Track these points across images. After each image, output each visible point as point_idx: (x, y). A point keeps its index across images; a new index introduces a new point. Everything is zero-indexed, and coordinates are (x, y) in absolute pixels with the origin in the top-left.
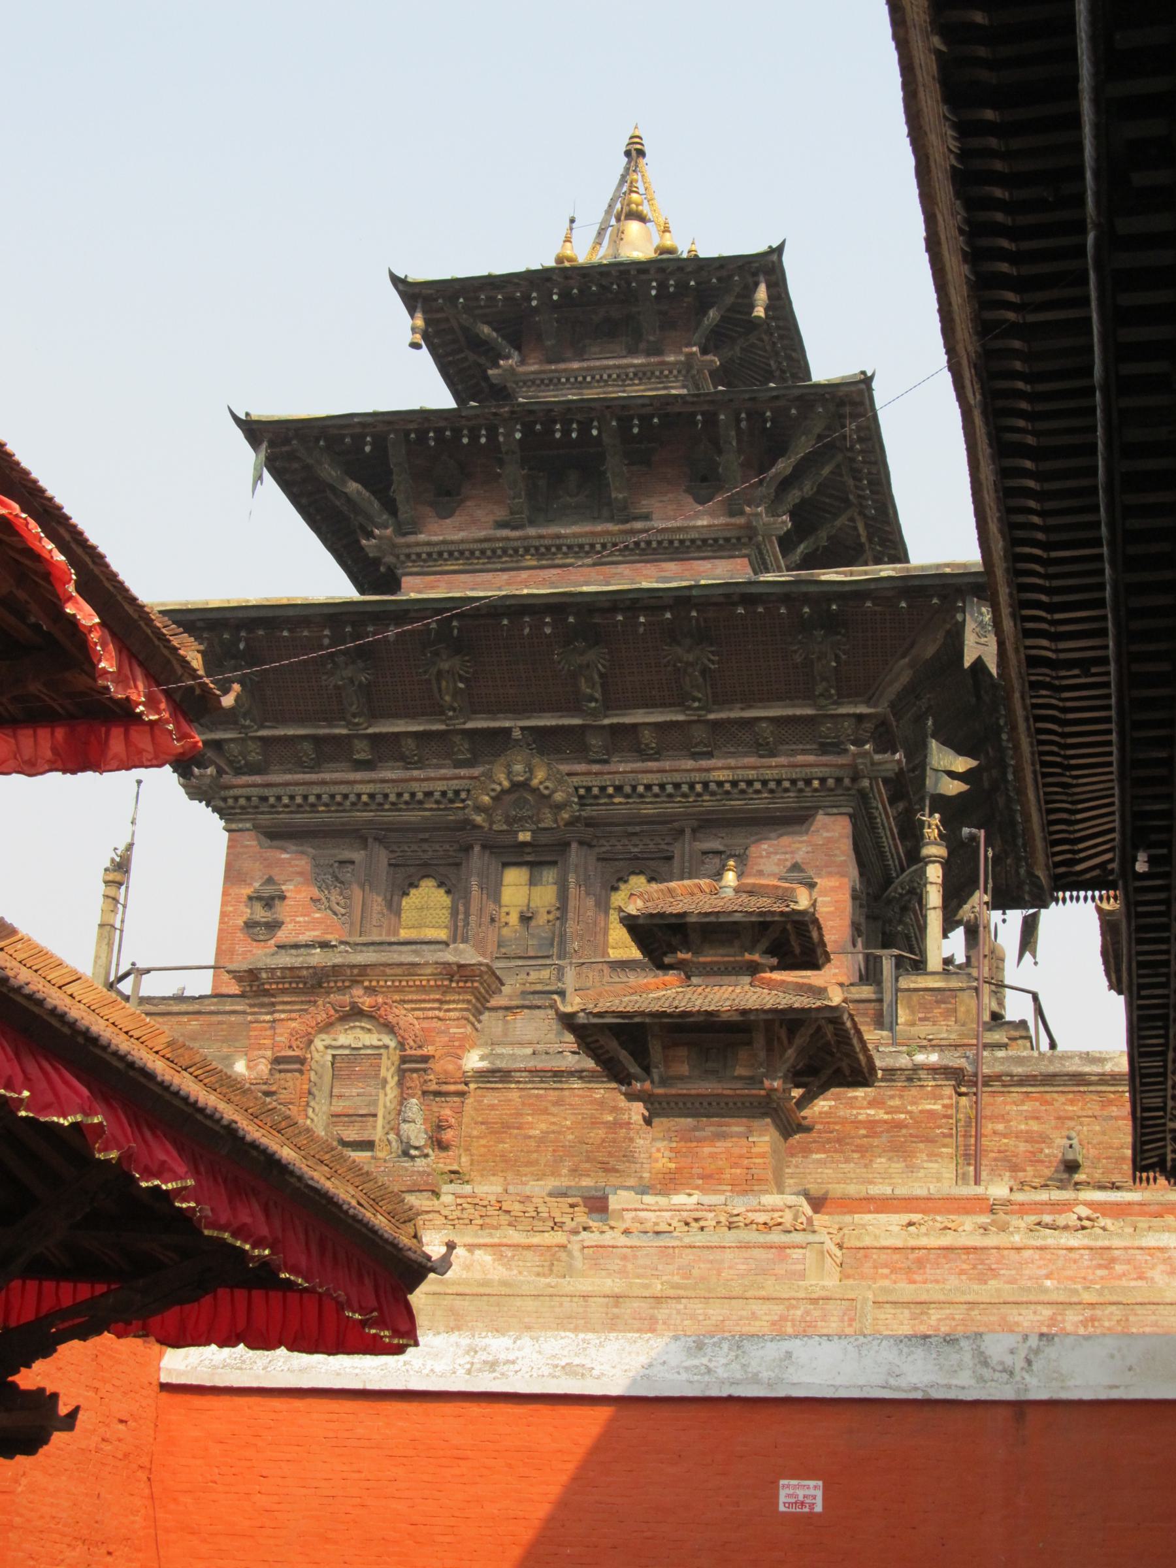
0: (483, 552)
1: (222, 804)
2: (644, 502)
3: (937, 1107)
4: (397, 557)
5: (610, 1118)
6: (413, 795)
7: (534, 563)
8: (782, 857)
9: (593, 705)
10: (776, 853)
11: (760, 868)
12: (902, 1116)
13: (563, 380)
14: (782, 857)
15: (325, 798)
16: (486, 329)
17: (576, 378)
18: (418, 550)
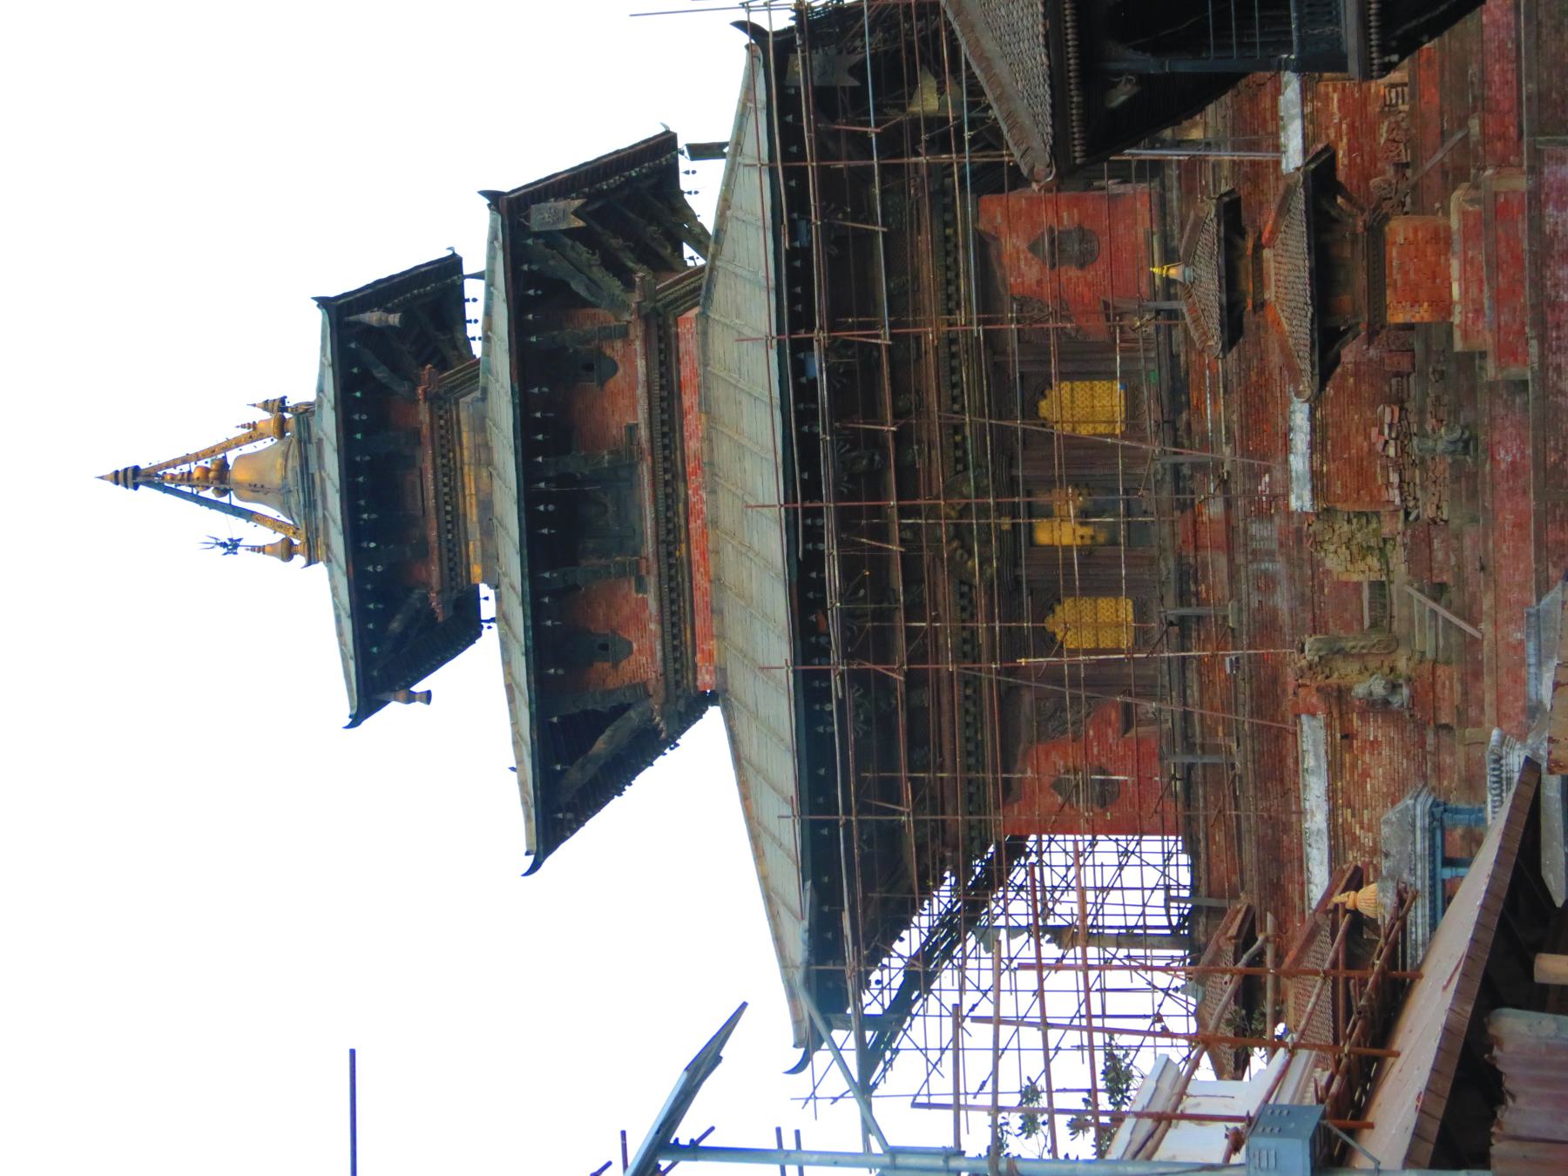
0: (672, 602)
1: (977, 843)
2: (614, 432)
3: (1336, 97)
4: (678, 698)
5: (1351, 380)
6: (965, 641)
7: (683, 546)
8: (1022, 262)
9: (877, 458)
10: (1019, 268)
11: (1034, 282)
12: (1344, 126)
13: (450, 536)
14: (1022, 262)
15: (970, 733)
16: (395, 625)
17: (448, 522)
18: (671, 674)
